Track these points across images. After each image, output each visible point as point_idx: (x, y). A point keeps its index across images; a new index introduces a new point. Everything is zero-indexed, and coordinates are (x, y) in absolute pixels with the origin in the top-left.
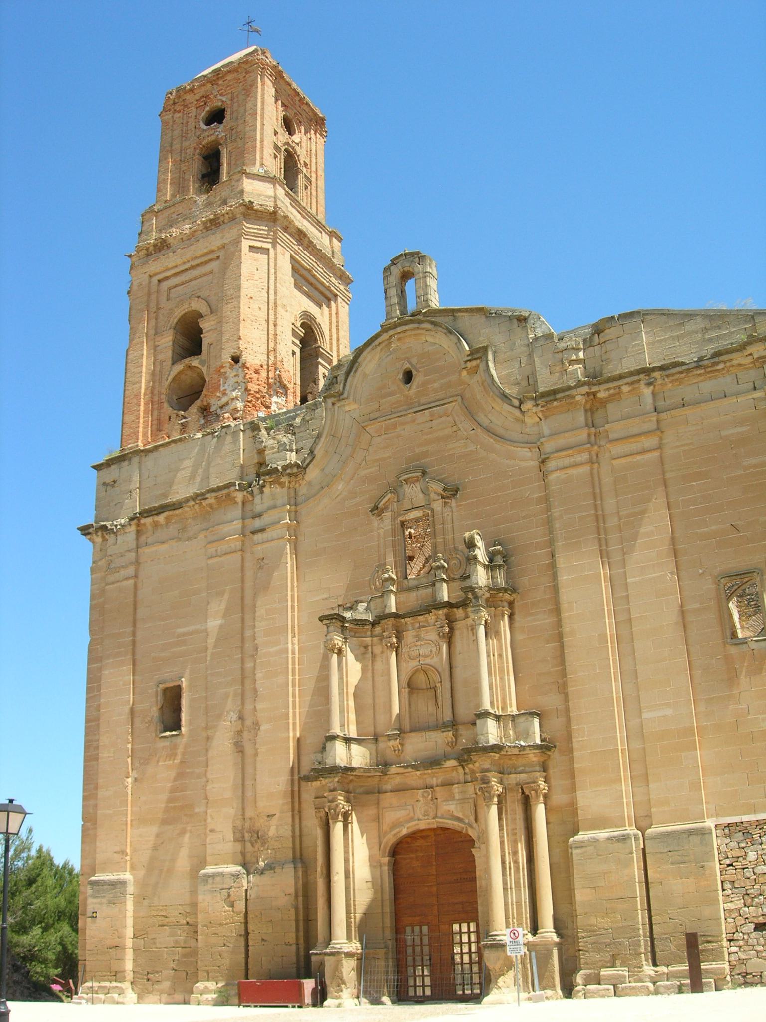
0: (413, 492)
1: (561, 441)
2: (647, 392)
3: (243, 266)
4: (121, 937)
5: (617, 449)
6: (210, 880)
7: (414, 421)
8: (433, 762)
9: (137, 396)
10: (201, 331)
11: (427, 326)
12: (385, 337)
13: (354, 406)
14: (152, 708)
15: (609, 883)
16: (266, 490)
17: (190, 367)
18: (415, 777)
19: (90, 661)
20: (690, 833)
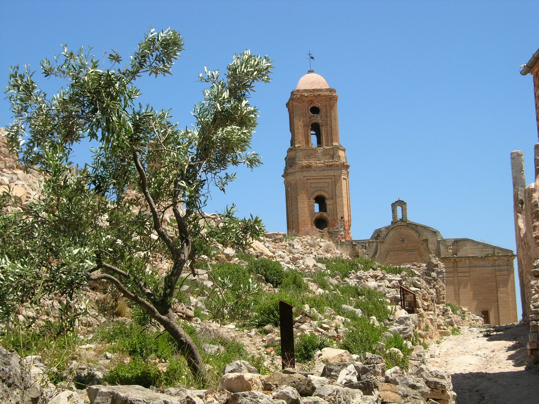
5: (460, 275)
7: (404, 254)
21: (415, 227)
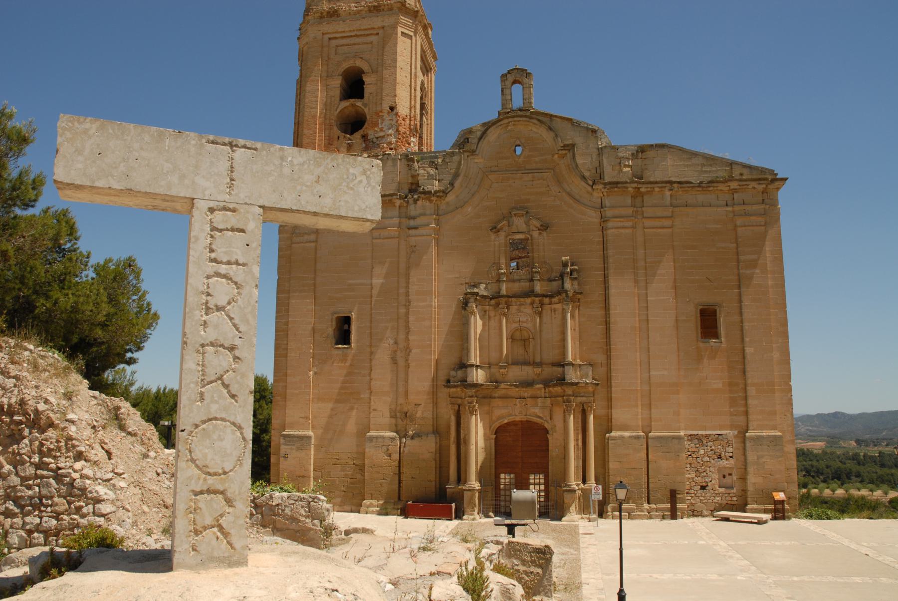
0: (519, 223)
1: (617, 212)
2: (668, 193)
3: (398, 45)
4: (308, 470)
5: (648, 223)
6: (374, 440)
8: (528, 384)
9: (314, 117)
10: (363, 83)
11: (535, 121)
12: (506, 121)
13: (482, 160)
14: (329, 329)
15: (626, 460)
16: (419, 203)
17: (353, 105)
18: (514, 392)
19: (279, 292)
20: (673, 437)
21: (546, 120)
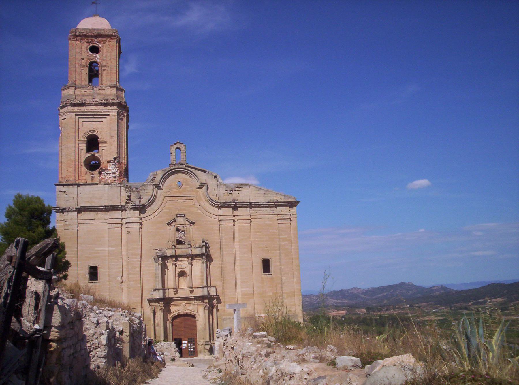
0: (180, 220)
